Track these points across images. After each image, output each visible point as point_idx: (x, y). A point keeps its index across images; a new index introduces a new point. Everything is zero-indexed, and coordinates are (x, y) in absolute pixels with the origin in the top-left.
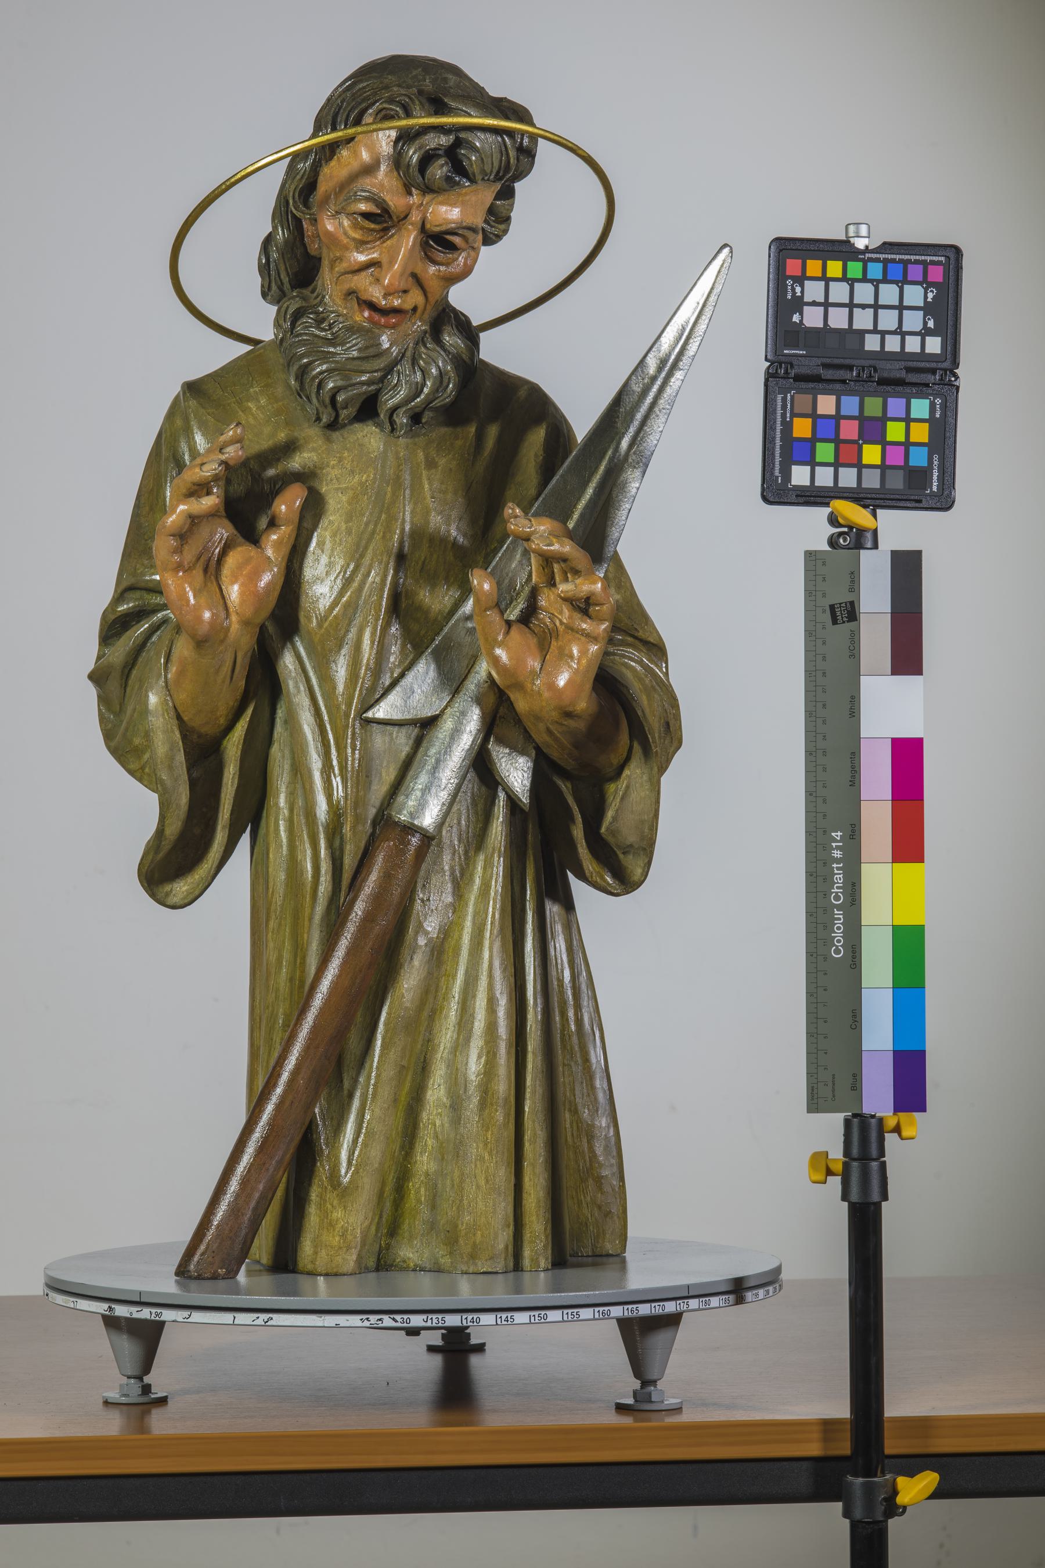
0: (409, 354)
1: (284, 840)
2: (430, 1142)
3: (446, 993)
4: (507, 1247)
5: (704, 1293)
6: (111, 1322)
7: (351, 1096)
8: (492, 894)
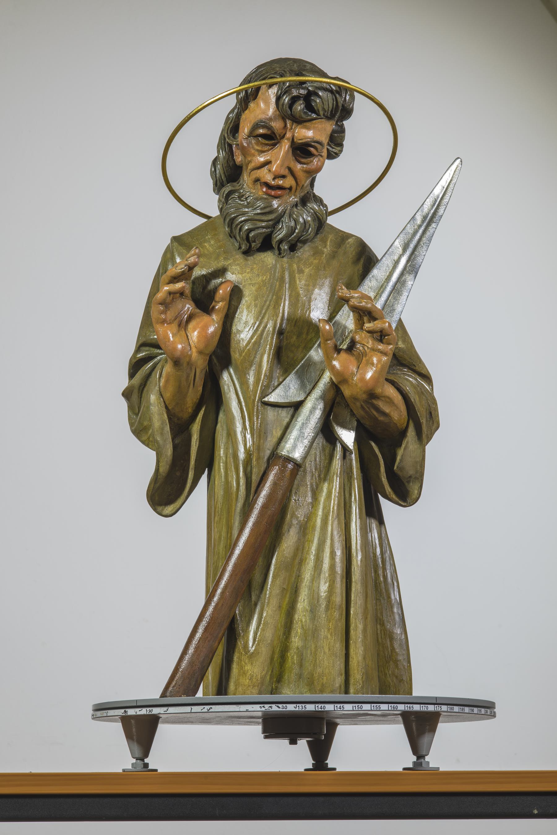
0: (287, 212)
1: (223, 474)
2: (299, 631)
3: (308, 551)
4: (340, 686)
7: (256, 605)
8: (333, 496)
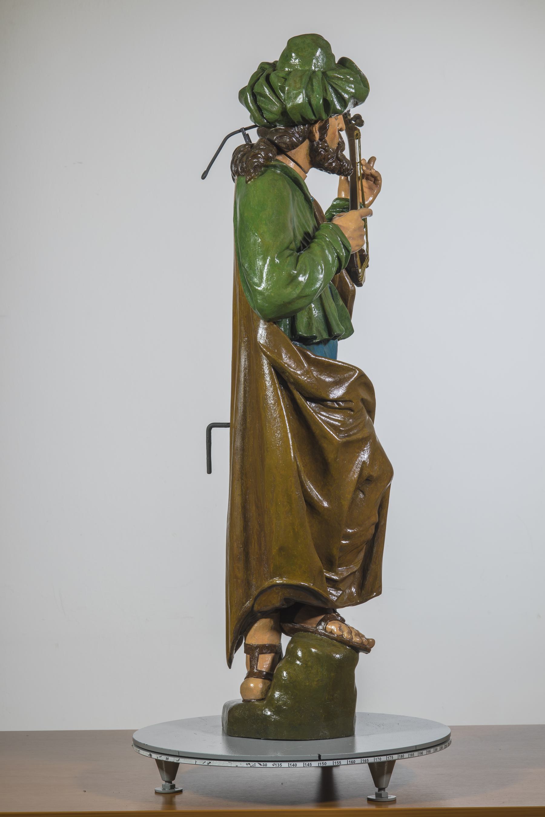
5: (401, 752)
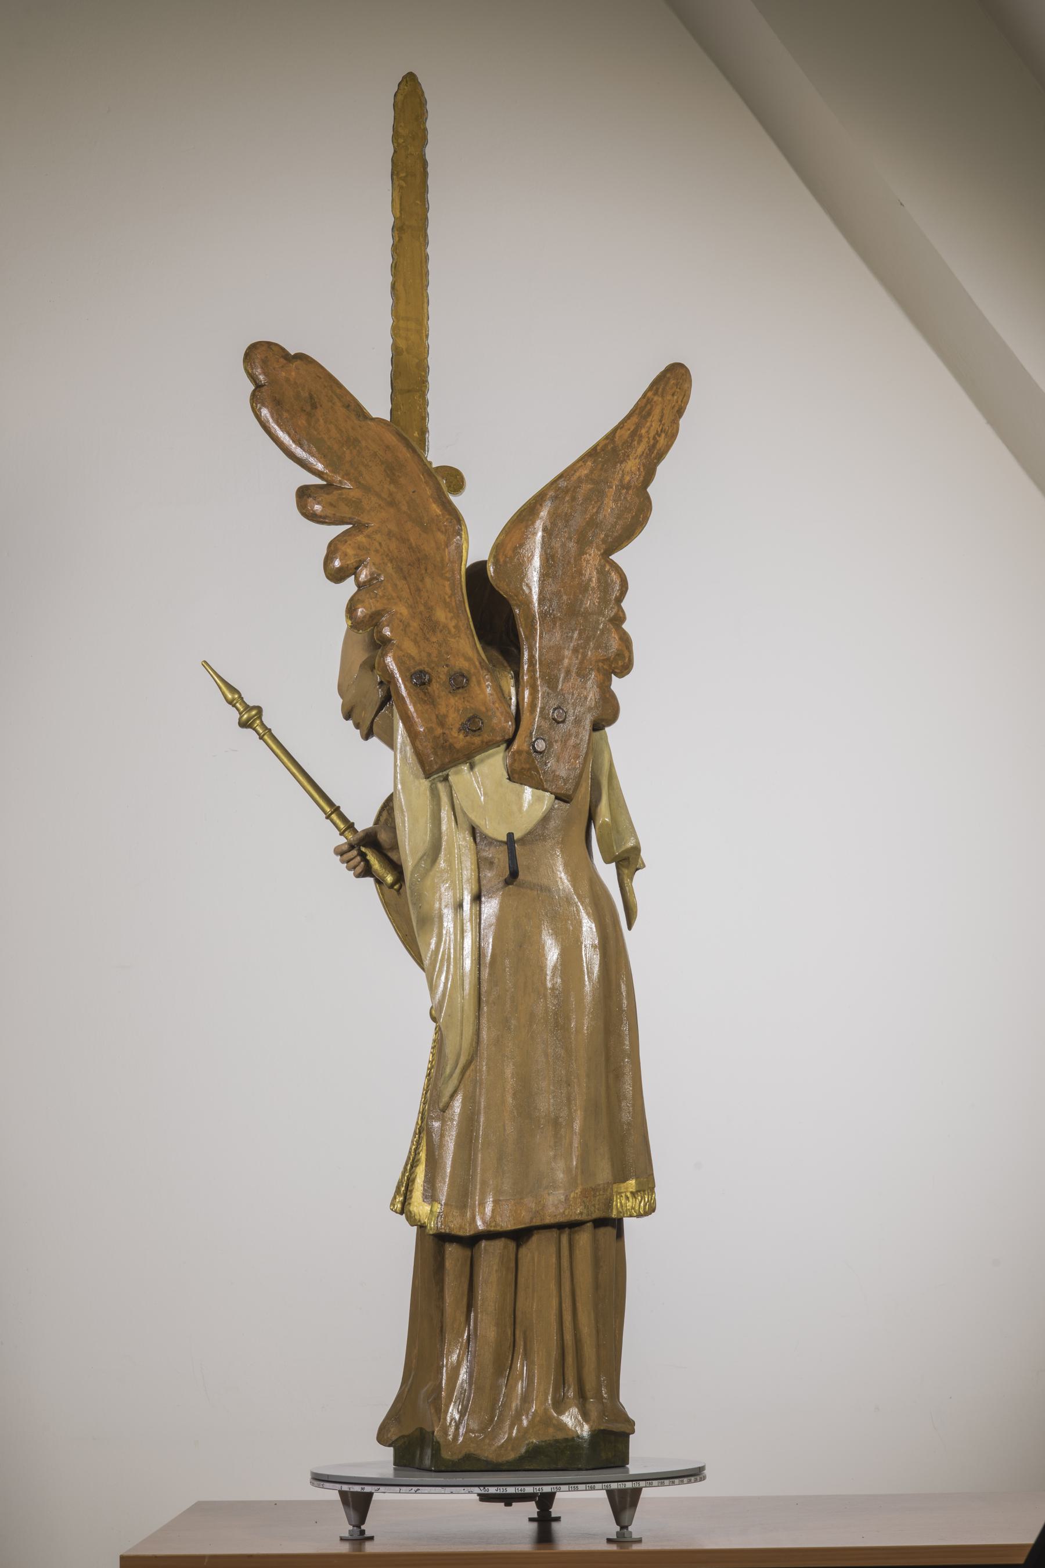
6: (342, 1493)
